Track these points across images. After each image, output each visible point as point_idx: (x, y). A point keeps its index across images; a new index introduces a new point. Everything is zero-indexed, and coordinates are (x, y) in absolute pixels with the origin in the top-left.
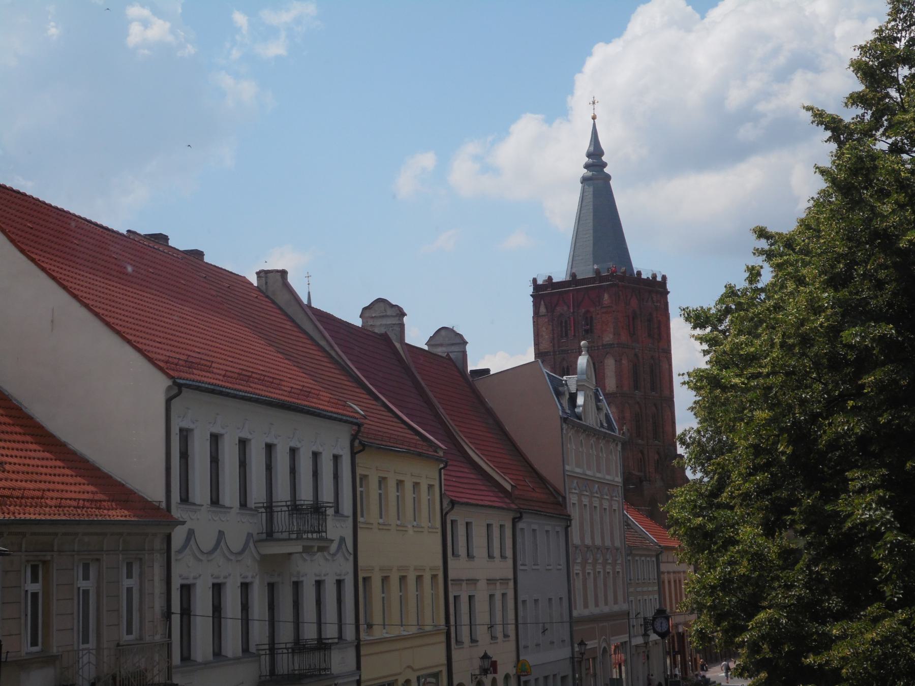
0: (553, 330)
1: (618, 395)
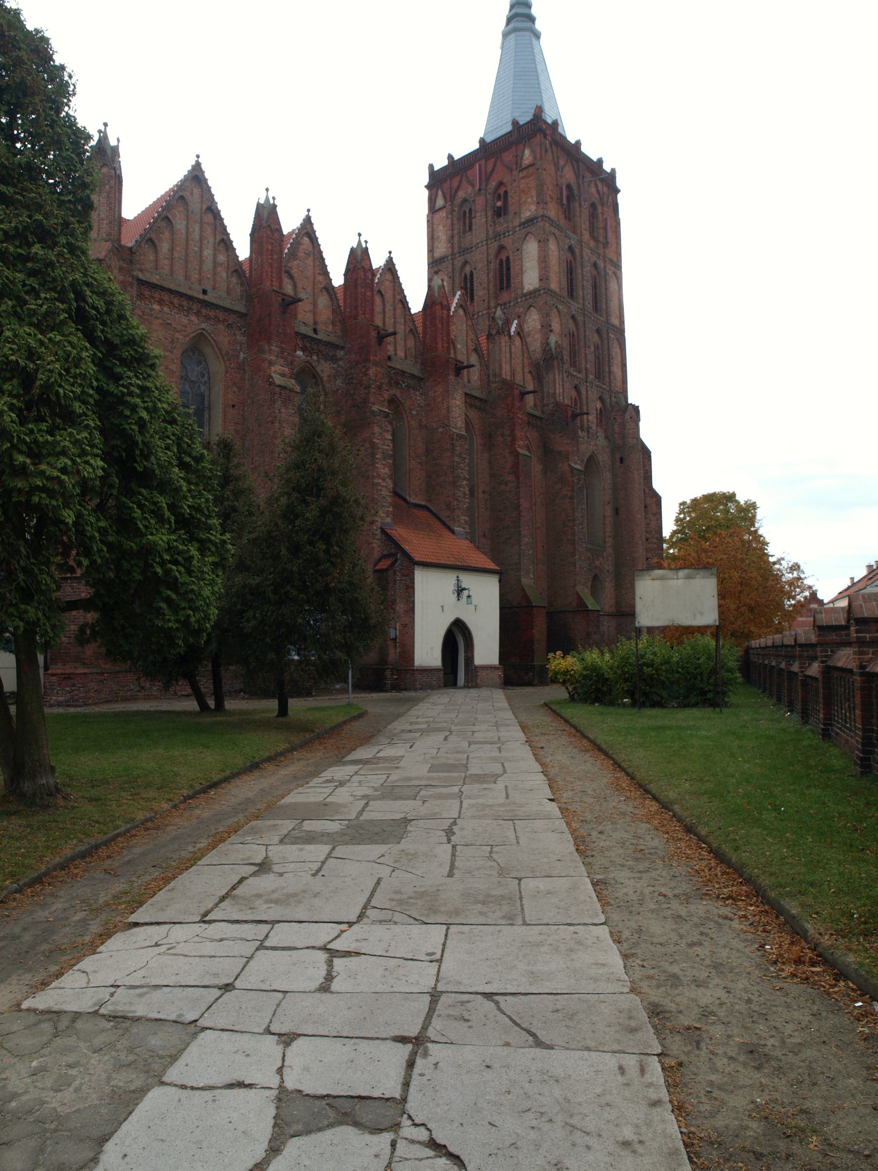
0: (452, 224)
1: (542, 292)
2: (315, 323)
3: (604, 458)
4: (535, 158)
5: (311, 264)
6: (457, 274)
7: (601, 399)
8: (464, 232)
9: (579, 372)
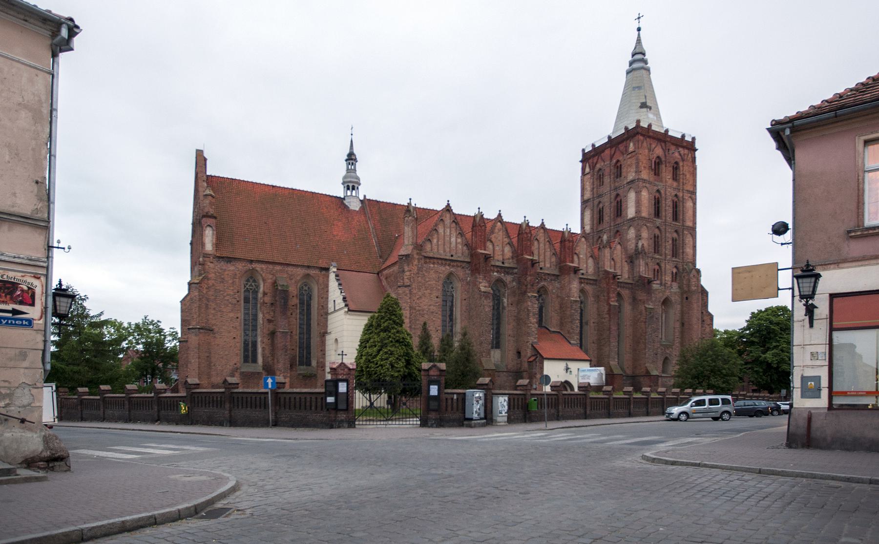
0: (593, 182)
2: (503, 259)
3: (675, 298)
4: (635, 148)
6: (595, 208)
7: (676, 267)
8: (600, 186)
9: (661, 256)
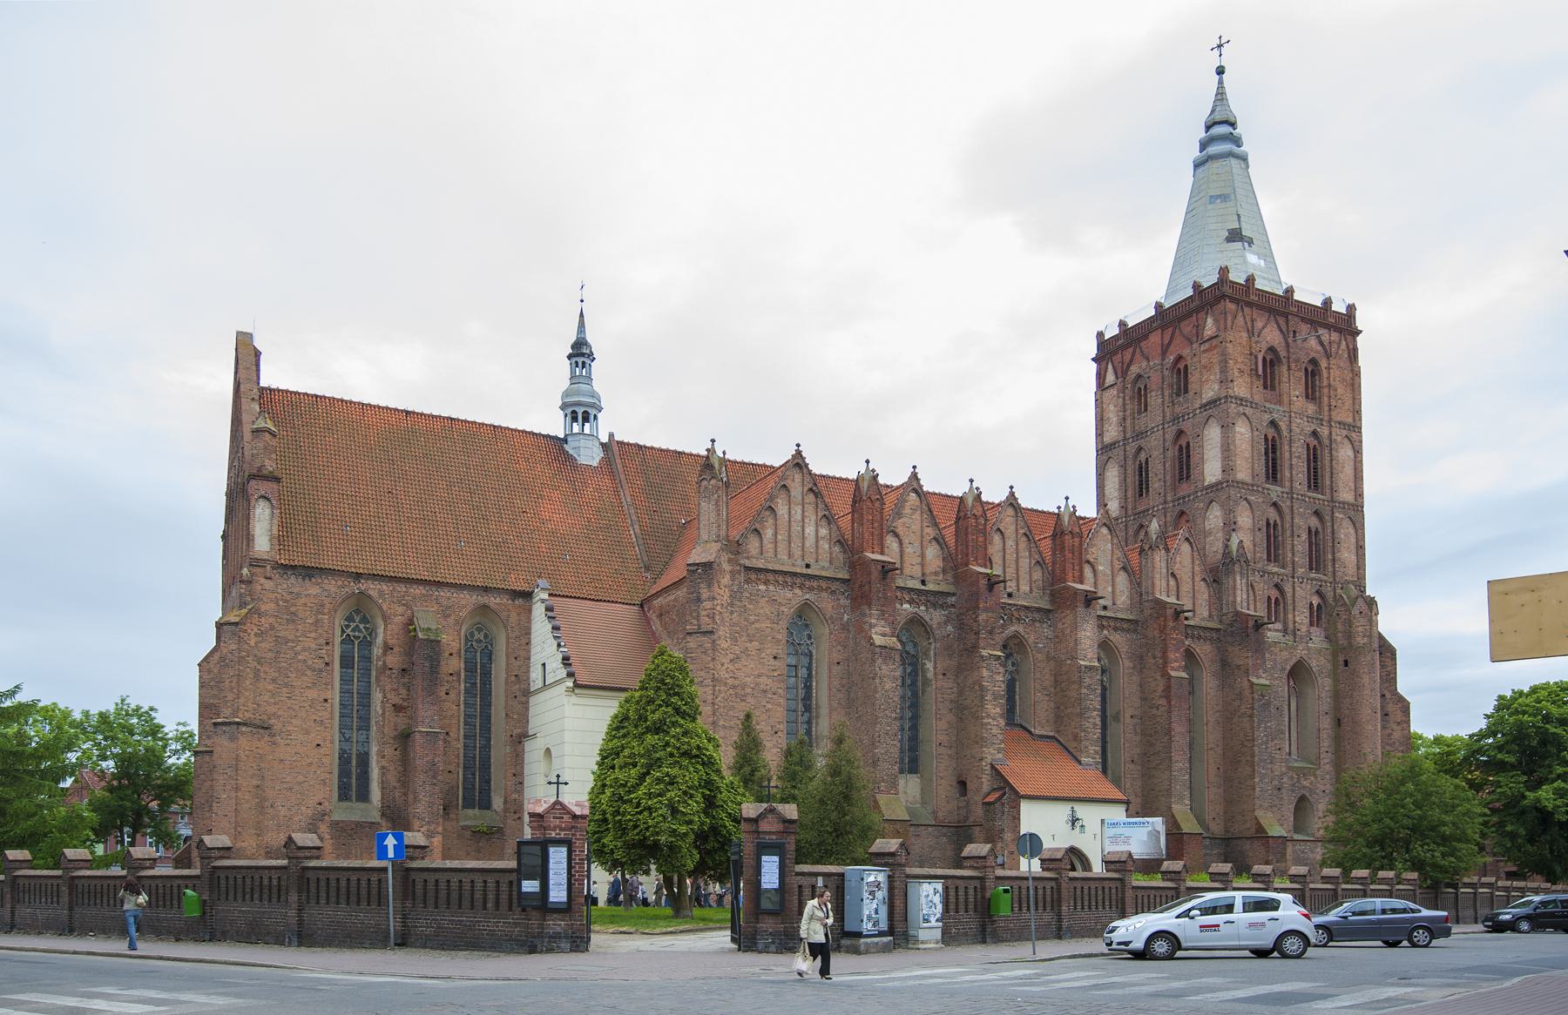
1: (1225, 485)
2: (923, 574)
5: (919, 518)
